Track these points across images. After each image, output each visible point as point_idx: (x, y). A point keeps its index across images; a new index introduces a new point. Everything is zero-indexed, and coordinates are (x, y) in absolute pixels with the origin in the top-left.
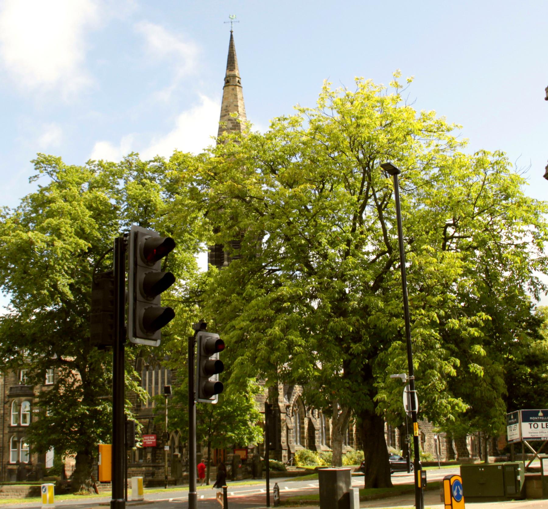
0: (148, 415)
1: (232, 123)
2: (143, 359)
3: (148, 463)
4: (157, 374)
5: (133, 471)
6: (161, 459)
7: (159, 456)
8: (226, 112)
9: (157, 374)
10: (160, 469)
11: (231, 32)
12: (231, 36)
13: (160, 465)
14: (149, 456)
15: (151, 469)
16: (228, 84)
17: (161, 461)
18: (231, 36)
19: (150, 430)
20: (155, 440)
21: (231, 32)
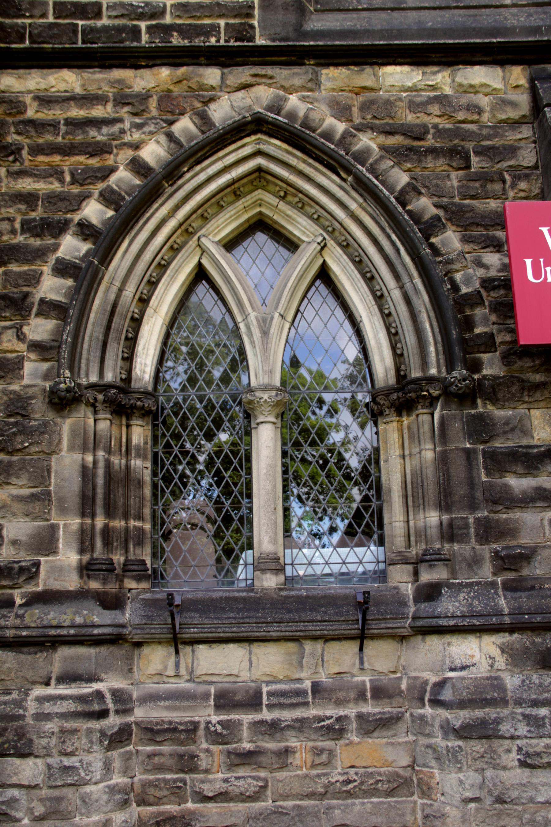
5: (225, 701)
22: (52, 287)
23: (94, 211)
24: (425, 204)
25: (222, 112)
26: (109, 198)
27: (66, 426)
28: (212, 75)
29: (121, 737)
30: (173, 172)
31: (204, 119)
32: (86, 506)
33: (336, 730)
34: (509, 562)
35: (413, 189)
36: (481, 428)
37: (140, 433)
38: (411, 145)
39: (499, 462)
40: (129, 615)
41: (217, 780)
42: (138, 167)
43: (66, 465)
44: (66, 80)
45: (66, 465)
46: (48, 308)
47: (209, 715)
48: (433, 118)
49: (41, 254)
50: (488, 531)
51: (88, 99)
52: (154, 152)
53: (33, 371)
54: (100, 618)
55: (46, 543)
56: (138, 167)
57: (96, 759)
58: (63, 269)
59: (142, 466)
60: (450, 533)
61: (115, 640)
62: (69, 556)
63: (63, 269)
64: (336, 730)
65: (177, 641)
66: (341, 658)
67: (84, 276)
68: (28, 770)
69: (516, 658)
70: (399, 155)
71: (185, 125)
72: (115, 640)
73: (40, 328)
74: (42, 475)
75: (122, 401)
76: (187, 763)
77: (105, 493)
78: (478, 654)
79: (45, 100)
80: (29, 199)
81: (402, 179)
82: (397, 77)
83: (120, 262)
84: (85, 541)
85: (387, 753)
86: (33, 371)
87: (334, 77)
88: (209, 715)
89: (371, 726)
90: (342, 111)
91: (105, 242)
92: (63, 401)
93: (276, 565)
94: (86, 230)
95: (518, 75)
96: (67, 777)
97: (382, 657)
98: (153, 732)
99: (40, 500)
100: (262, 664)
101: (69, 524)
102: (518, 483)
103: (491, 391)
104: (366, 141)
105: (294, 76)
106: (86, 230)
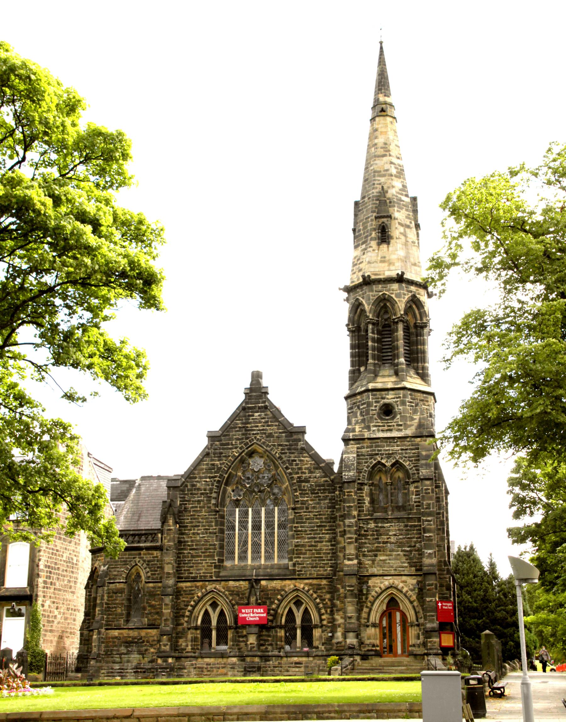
0: (244, 576)
1: (396, 168)
2: (229, 489)
3: (251, 651)
4: (257, 513)
5: (207, 664)
6: (271, 645)
7: (268, 640)
8: (386, 151)
9: (257, 513)
10: (269, 661)
11: (381, 43)
12: (381, 48)
13: (270, 654)
14: (252, 640)
15: (257, 660)
16: (383, 113)
17: (270, 648)
18: (381, 48)
19: (253, 599)
20: (265, 615)
21: (381, 43)
22: (187, 613)
23: (192, 603)
24: (233, 602)
25: (208, 588)
26: (194, 601)
27: (189, 632)
28: (207, 583)
29: (195, 668)
30: (202, 598)
31: (206, 590)
32: (192, 641)
33: (219, 668)
34: (239, 649)
35: (232, 600)
36: (237, 632)
37: (198, 632)
38: (232, 593)
39: (239, 637)
40: (196, 654)
41: (206, 673)
42: (198, 597)
43: (190, 636)
44: (189, 584)
45: (190, 636)
46: (187, 616)
47: (205, 666)
48: (235, 589)
49: (186, 609)
50: (237, 645)
51: (191, 587)
52: (200, 594)
53: (185, 624)
54: (193, 655)
55: (187, 646)
56: (198, 597)
57: (192, 670)
58: (189, 611)
59: (199, 636)
60: (233, 645)
61: (194, 657)
62: (190, 647)
63: (189, 611)
64: (219, 668)
65: (202, 657)
66: (220, 660)
67: (191, 612)
68: (186, 671)
69: (238, 660)
70: (231, 595)
71: (204, 590)
72: (194, 657)
73: (186, 619)
74: (186, 638)
75: (196, 628)
76: (202, 671)
77: (194, 639)
78: (234, 660)
79: (186, 587)
80: (184, 601)
81: (231, 598)
82: (231, 583)
83: (196, 610)
84: (192, 646)
85: (224, 671)
86: (185, 624)
87: (223, 583)
88: (205, 666)
89: (223, 668)
90: (224, 588)
91: (194, 607)
92: (189, 629)
93: (214, 648)
94: (191, 606)
95: (247, 582)
96: (189, 672)
97: (225, 660)
98: (199, 668)
99: (186, 641)
100: (211, 660)
101: (190, 644)
102: (241, 639)
103: (239, 628)
104: (227, 593)
105: (218, 583)
106: (191, 606)
